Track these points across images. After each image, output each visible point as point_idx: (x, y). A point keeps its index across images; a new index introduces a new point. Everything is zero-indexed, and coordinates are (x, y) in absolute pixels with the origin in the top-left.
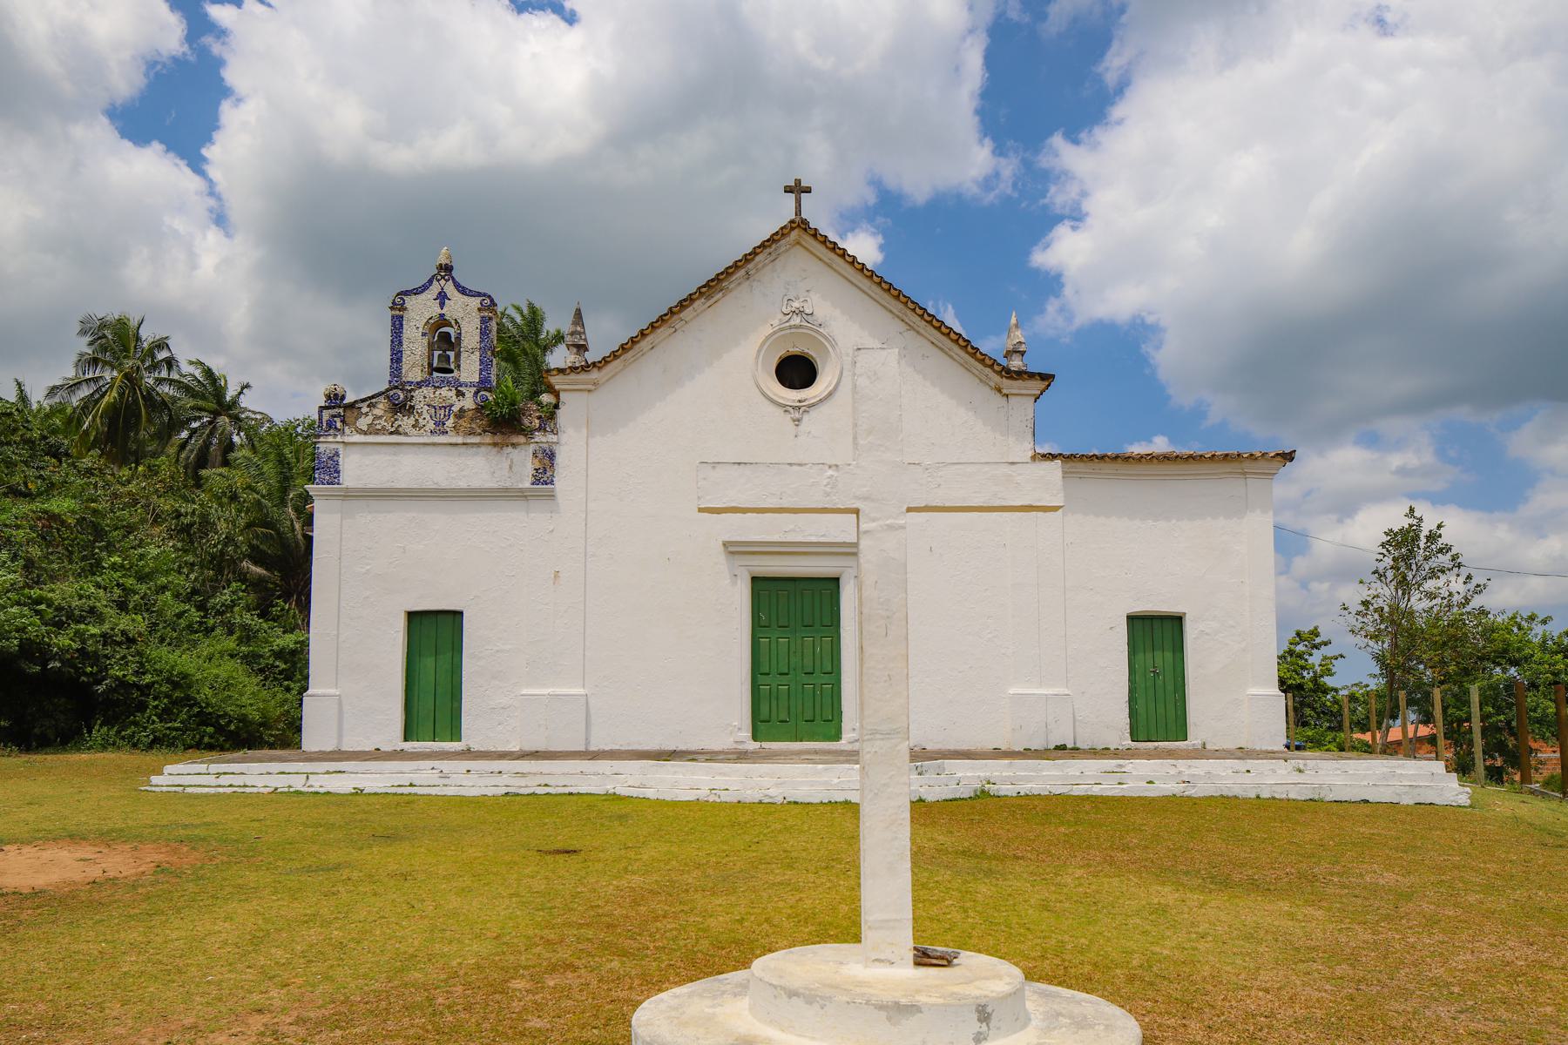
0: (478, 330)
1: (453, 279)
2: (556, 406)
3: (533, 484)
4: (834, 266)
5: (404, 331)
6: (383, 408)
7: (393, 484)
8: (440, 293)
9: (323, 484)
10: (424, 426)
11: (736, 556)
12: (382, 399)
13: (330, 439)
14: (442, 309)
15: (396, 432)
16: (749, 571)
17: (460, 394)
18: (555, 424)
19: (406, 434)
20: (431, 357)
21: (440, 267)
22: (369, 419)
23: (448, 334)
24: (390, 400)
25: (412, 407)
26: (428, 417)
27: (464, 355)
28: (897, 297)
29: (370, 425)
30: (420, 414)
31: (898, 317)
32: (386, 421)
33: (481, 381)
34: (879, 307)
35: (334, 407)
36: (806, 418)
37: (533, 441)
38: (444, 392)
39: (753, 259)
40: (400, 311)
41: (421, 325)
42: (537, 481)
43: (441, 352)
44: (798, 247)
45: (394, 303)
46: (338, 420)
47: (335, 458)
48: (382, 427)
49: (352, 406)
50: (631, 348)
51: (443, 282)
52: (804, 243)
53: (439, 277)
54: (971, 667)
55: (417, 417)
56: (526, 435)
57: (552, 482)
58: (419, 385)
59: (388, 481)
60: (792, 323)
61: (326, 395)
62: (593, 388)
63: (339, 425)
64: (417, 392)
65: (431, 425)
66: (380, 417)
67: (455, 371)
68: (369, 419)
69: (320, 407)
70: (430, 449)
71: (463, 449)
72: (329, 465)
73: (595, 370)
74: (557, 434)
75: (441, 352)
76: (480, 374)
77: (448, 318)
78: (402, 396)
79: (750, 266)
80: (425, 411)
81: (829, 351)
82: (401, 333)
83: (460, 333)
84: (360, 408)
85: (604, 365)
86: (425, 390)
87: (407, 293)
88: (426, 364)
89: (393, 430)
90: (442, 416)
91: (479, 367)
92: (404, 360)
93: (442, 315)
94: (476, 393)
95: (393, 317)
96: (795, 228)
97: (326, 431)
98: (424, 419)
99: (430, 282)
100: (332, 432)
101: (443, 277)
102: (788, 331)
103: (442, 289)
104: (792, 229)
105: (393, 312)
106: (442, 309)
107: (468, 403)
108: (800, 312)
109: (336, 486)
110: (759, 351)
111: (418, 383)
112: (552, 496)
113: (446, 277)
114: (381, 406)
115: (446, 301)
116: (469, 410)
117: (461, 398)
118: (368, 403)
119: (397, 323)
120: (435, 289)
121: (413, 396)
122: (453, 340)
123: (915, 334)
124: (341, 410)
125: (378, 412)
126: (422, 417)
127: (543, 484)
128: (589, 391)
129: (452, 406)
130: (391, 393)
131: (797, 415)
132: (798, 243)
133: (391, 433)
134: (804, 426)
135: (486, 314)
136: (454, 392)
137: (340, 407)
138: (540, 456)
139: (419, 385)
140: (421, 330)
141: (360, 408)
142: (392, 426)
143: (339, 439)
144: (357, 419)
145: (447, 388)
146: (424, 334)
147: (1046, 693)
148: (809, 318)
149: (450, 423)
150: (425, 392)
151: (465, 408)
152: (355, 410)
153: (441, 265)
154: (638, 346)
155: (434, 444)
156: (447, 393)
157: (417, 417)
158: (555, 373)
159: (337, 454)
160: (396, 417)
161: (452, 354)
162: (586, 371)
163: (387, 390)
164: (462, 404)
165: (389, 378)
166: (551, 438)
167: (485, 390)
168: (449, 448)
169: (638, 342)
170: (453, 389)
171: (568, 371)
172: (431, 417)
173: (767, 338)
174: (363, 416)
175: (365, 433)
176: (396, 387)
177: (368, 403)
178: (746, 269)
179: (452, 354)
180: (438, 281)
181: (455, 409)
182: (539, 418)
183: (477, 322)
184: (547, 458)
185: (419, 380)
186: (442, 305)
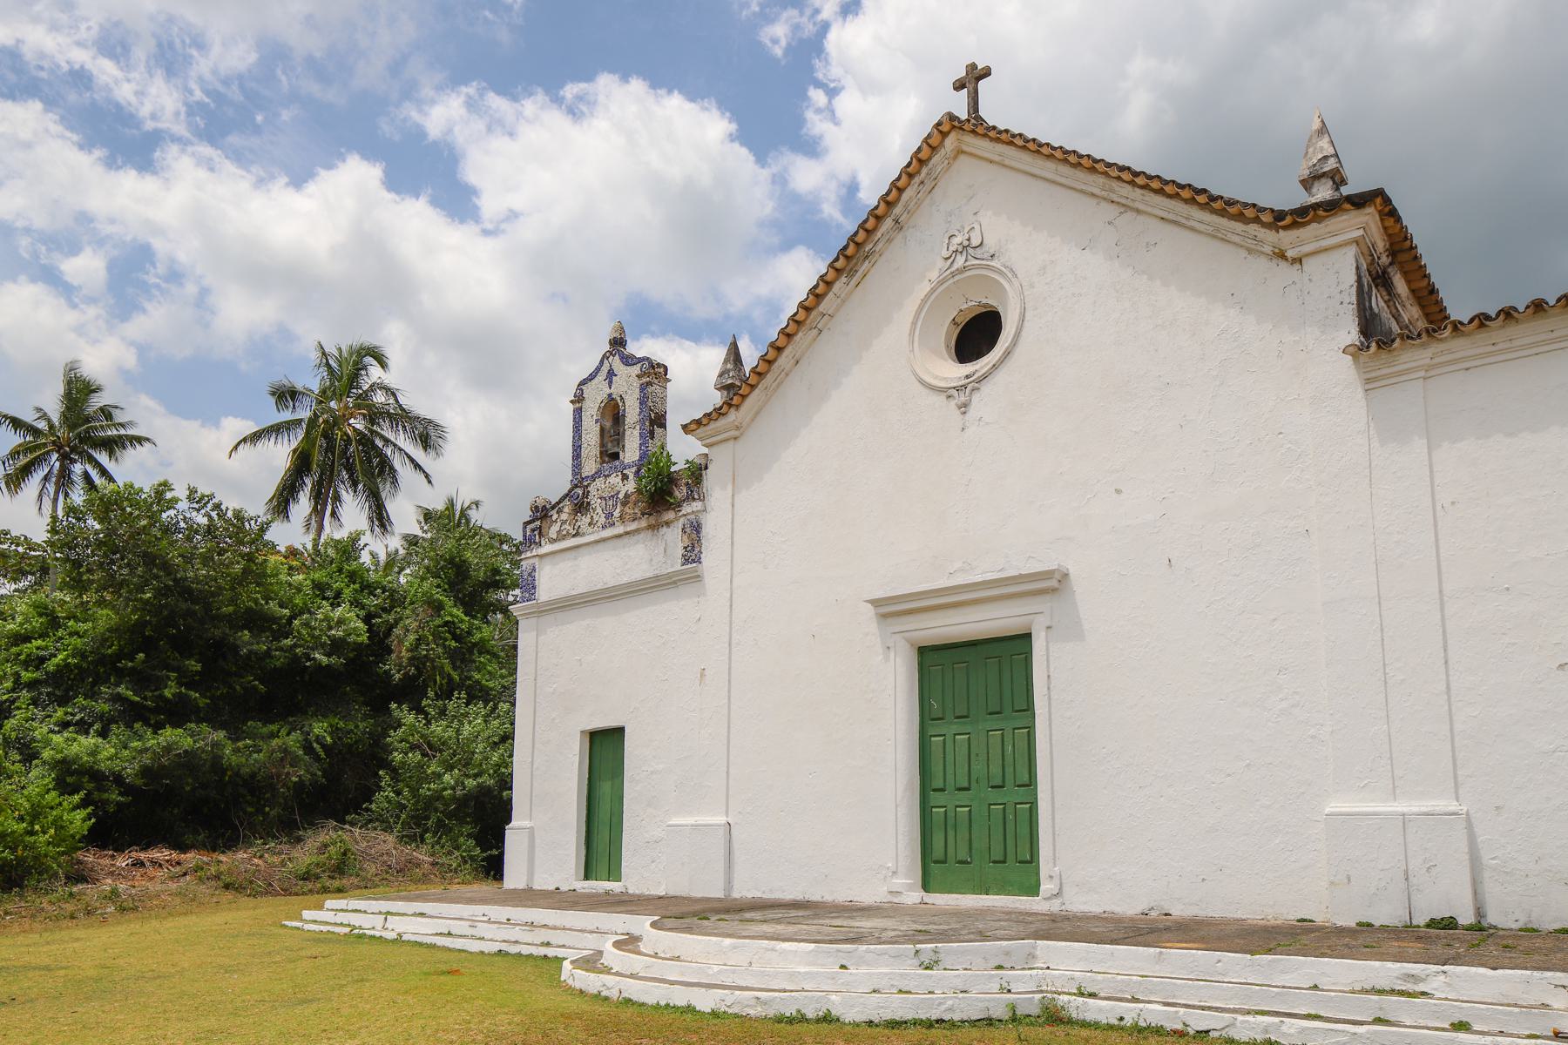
4: (1007, 162)
11: (889, 620)
16: (908, 640)
17: (625, 477)
25: (588, 503)
28: (1093, 170)
30: (594, 510)
31: (1105, 199)
32: (570, 524)
34: (1076, 195)
36: (976, 397)
37: (681, 514)
39: (898, 199)
42: (686, 560)
44: (962, 157)
48: (567, 532)
52: (965, 148)
54: (1248, 765)
56: (674, 509)
60: (955, 267)
65: (603, 520)
70: (600, 546)
71: (626, 540)
79: (897, 210)
81: (1004, 288)
86: (599, 483)
96: (949, 132)
102: (951, 281)
104: (944, 135)
107: (631, 486)
108: (965, 248)
110: (914, 324)
112: (698, 578)
123: (1135, 214)
125: (564, 516)
128: (735, 438)
129: (618, 492)
131: (963, 399)
132: (960, 152)
134: (973, 412)
136: (620, 476)
138: (688, 530)
139: (593, 478)
147: (1405, 810)
148: (978, 253)
149: (617, 514)
151: (629, 492)
155: (604, 540)
156: (615, 479)
163: (570, 491)
164: (626, 488)
166: (697, 506)
168: (615, 540)
173: (924, 301)
176: (576, 486)
178: (893, 217)
181: (621, 496)
184: (695, 530)
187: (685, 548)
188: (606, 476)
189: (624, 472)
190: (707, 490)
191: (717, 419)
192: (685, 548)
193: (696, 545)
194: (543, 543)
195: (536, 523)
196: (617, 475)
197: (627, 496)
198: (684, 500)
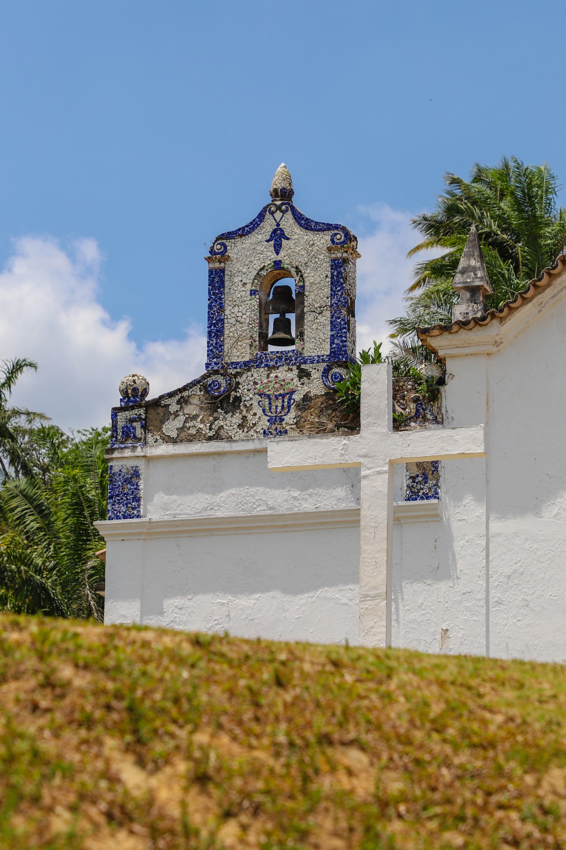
0: (329, 280)
1: (293, 209)
2: (442, 381)
3: (408, 499)
5: (227, 290)
6: (199, 403)
7: (212, 512)
8: (274, 231)
9: (118, 518)
10: (254, 425)
12: (196, 390)
13: (128, 453)
14: (278, 253)
15: (217, 437)
17: (304, 374)
18: (440, 408)
19: (229, 439)
20: (263, 324)
21: (275, 193)
22: (178, 422)
23: (287, 289)
24: (207, 392)
25: (238, 399)
26: (260, 412)
27: (309, 318)
29: (181, 430)
30: (249, 408)
32: (202, 421)
33: (334, 353)
35: (133, 408)
38: (282, 373)
40: (220, 262)
41: (248, 279)
43: (278, 316)
45: (212, 252)
46: (137, 425)
47: (134, 480)
49: (156, 403)
50: (548, 285)
51: (278, 215)
53: (273, 209)
55: (244, 413)
57: (436, 496)
58: (247, 366)
59: (206, 509)
61: (121, 391)
62: (494, 349)
63: (139, 432)
64: (244, 376)
65: (264, 423)
66: (195, 417)
67: (297, 341)
68: (178, 422)
69: (114, 409)
72: (126, 491)
73: (495, 322)
74: (442, 423)
75: (278, 316)
76: (332, 343)
77: (286, 266)
78: (224, 384)
80: (255, 404)
82: (222, 293)
83: (303, 287)
84: (167, 406)
85: (508, 315)
86: (260, 374)
87: (229, 236)
88: (256, 336)
89: (211, 434)
90: (279, 408)
91: (330, 333)
92: (226, 332)
93: (277, 264)
94: (326, 372)
95: (211, 272)
97: (122, 443)
98: (255, 414)
99: (261, 216)
100: (129, 443)
101: (279, 208)
103: (278, 225)
105: (211, 265)
106: (278, 253)
109: (135, 520)
111: (246, 364)
113: (284, 208)
114: (195, 401)
115: (284, 242)
116: (316, 396)
117: (305, 379)
118: (178, 397)
119: (216, 280)
120: (268, 225)
121: (238, 383)
122: (294, 296)
124: (142, 411)
125: (191, 409)
126: (252, 413)
127: (422, 498)
129: (292, 392)
130: (209, 380)
133: (210, 439)
135: (339, 255)
136: (296, 372)
137: (140, 406)
139: (247, 366)
140: (249, 287)
141: (167, 406)
142: (210, 429)
143: (139, 452)
144: (162, 422)
145: (286, 368)
146: (253, 293)
149: (290, 418)
150: (255, 375)
151: (312, 394)
152: (161, 410)
153: (275, 190)
154: (559, 280)
157: (244, 413)
158: (436, 332)
159: (136, 474)
160: (215, 415)
161: (292, 317)
162: (481, 325)
163: (204, 377)
164: (306, 389)
165: (205, 360)
167: (340, 366)
169: (559, 274)
170: (294, 368)
171: (455, 328)
172: (264, 411)
174: (172, 417)
175: (174, 441)
176: (216, 372)
177: (178, 397)
179: (292, 317)
180: (272, 213)
181: (297, 397)
182: (416, 400)
183: (326, 269)
185: (247, 359)
186: (278, 248)
187: (413, 478)
188: (270, 368)
189: (303, 366)
190: (447, 411)
191: (457, 332)
192: (413, 478)
193: (430, 476)
194: (150, 438)
195: (136, 411)
196: (291, 370)
197: (306, 398)
198: (410, 419)
